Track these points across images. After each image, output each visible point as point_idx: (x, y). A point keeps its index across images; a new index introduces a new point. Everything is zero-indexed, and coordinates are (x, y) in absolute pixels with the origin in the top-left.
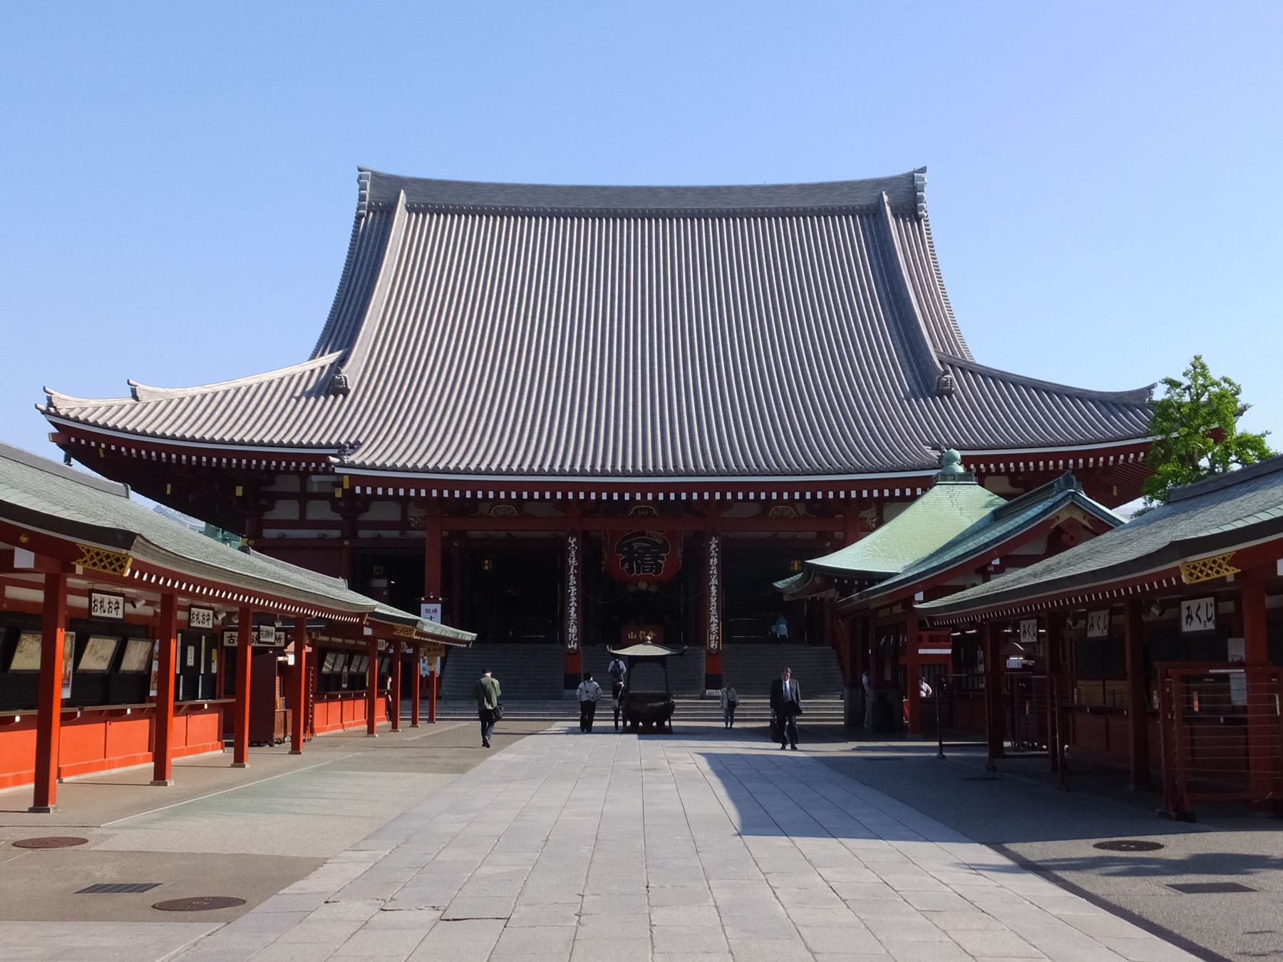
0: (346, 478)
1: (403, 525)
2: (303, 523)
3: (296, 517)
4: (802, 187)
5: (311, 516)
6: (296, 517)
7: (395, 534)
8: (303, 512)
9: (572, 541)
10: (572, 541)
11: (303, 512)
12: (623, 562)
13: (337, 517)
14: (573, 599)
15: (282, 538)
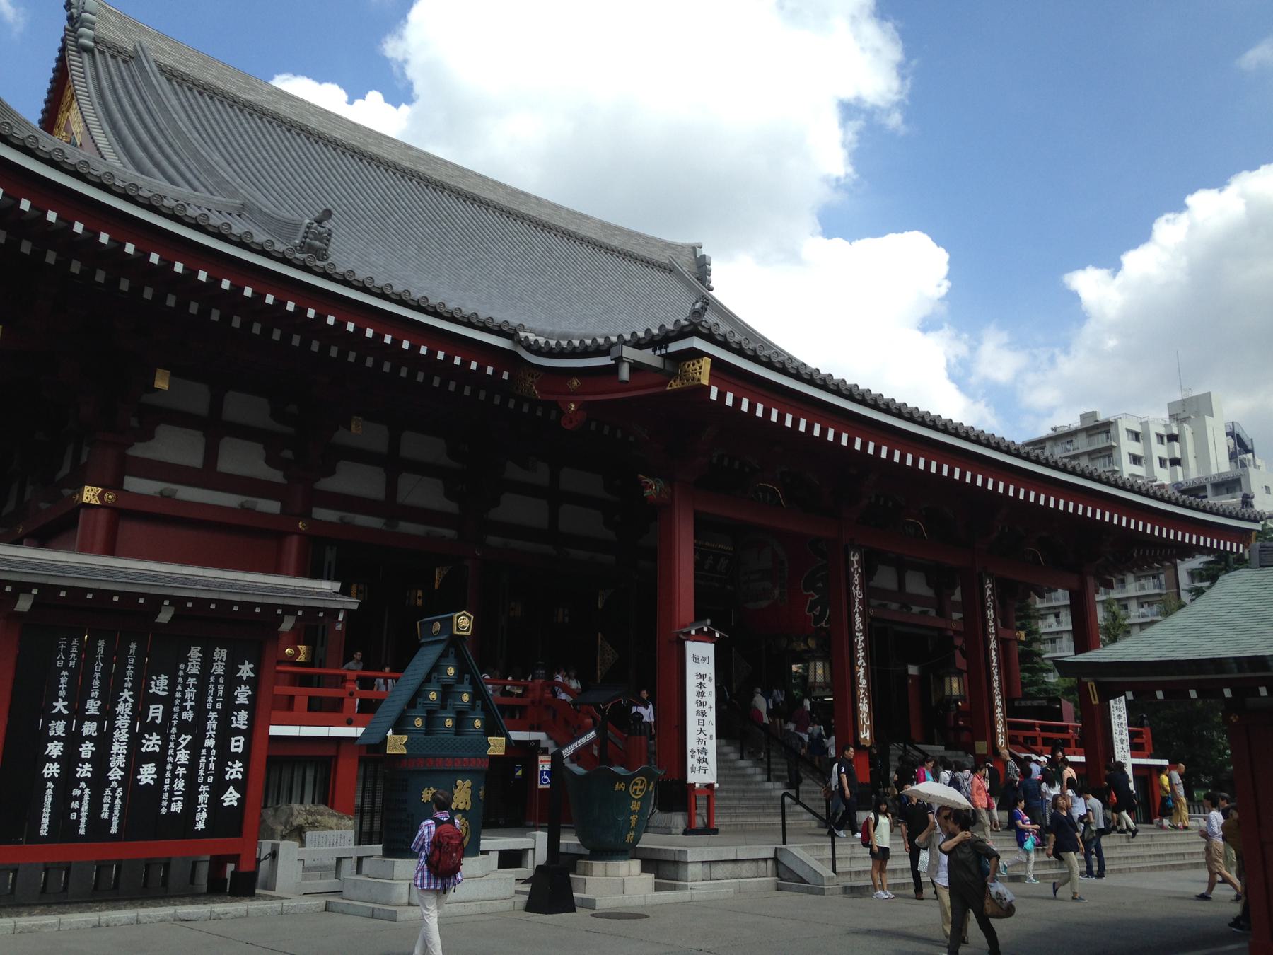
0: (706, 363)
1: (389, 508)
2: (207, 476)
3: (194, 459)
4: (604, 226)
5: (227, 464)
6: (194, 459)
7: (375, 522)
8: (211, 455)
9: (855, 558)
10: (855, 558)
11: (211, 455)
12: (813, 605)
13: (277, 476)
14: (861, 654)
15: (165, 497)
